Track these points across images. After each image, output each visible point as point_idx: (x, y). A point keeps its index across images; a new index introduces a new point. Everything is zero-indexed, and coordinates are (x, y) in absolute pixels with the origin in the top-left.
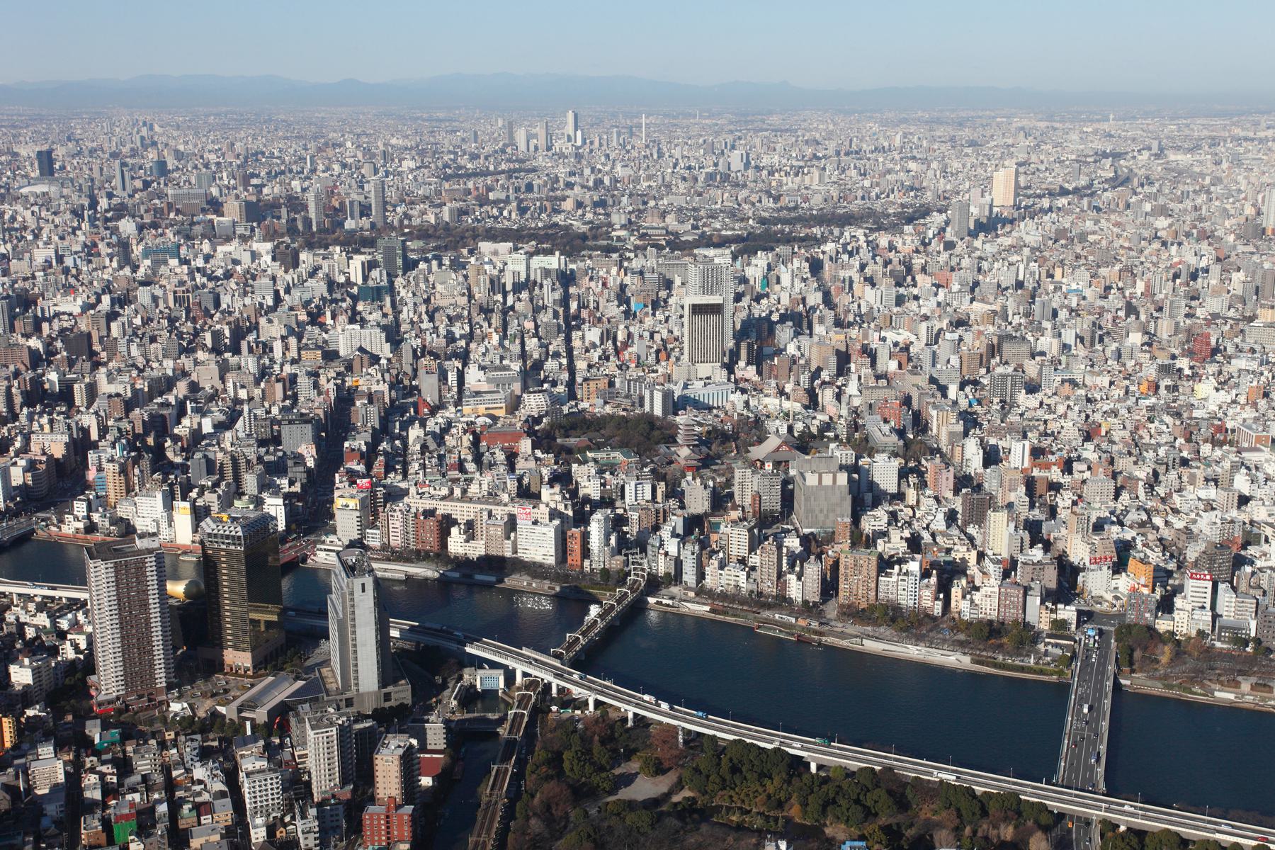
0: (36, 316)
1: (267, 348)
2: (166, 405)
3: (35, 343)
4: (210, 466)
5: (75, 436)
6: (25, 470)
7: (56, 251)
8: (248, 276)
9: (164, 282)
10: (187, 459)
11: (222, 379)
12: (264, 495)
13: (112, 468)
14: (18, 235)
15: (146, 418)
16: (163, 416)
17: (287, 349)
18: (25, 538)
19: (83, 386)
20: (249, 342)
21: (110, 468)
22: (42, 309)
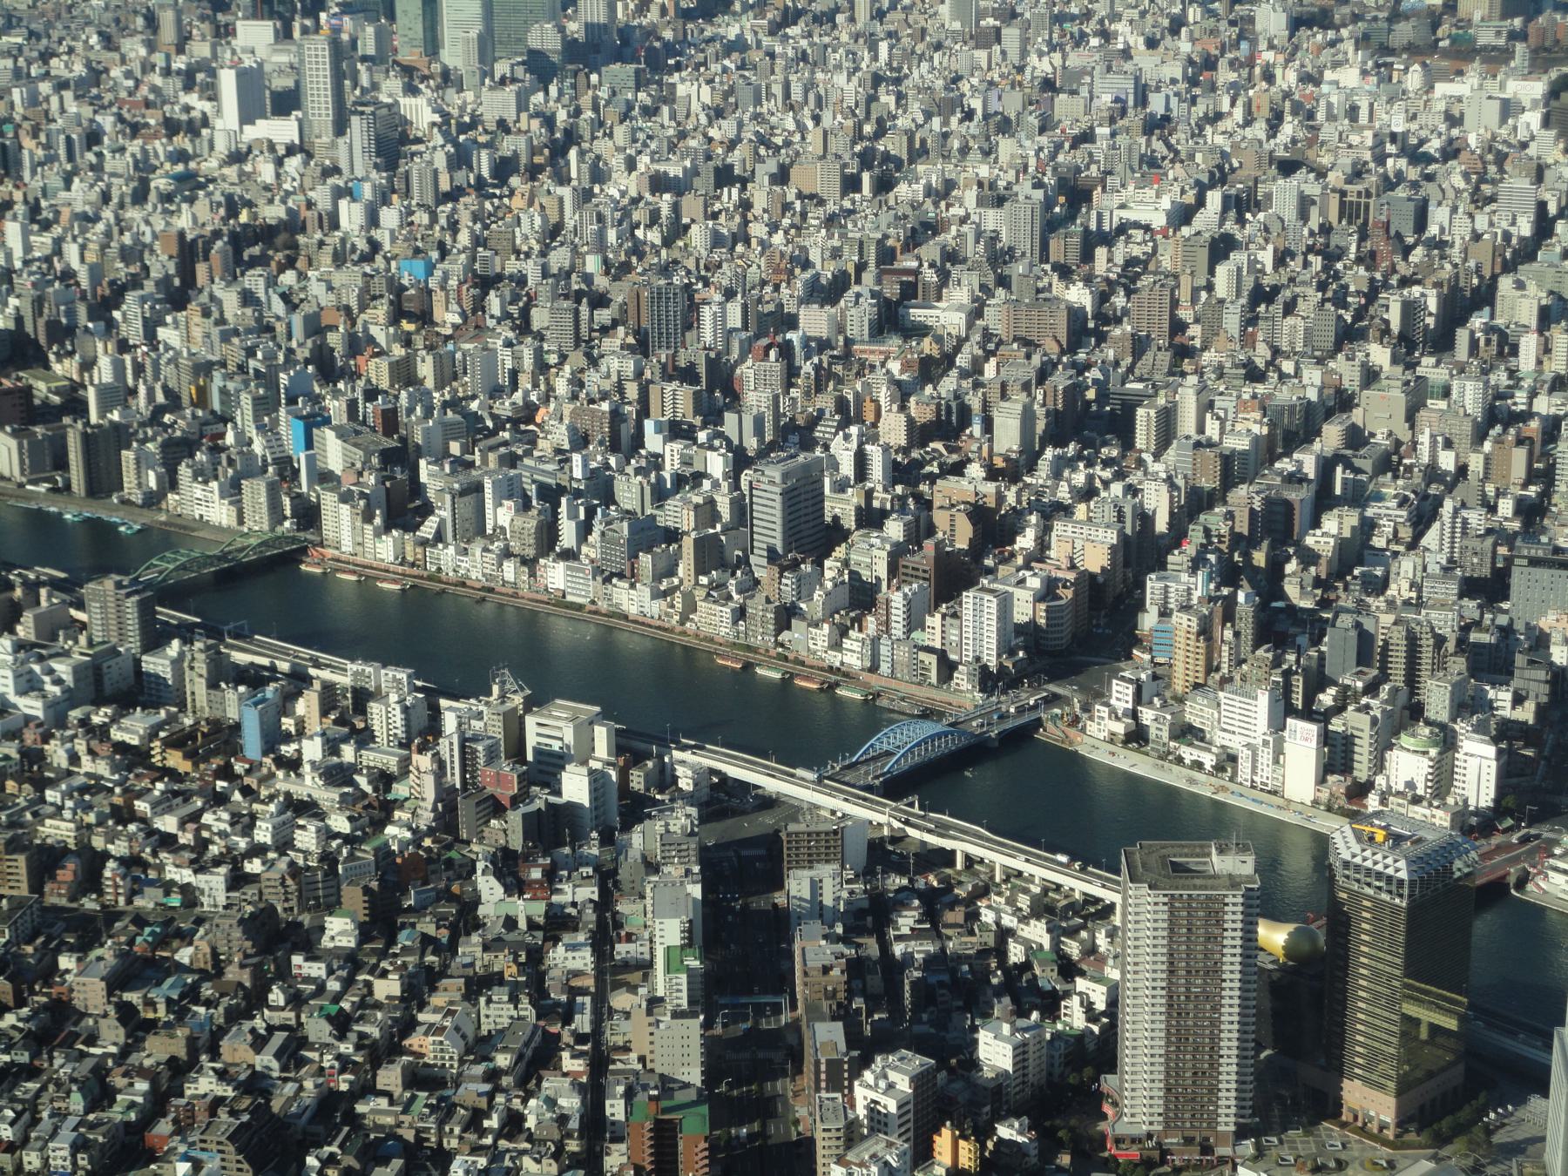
0: (1086, 230)
1: (1507, 347)
2: (1296, 479)
3: (1079, 295)
4: (1366, 648)
5: (1128, 531)
6: (1040, 598)
7: (1137, 79)
8: (1490, 157)
9: (1326, 160)
10: (1324, 604)
11: (1411, 418)
12: (1461, 727)
13: (1185, 623)
14: (1075, 29)
15: (1257, 506)
16: (1288, 506)
17: (1547, 350)
18: (1022, 737)
19: (1153, 413)
20: (1472, 333)
21: (1184, 623)
22: (1100, 217)
